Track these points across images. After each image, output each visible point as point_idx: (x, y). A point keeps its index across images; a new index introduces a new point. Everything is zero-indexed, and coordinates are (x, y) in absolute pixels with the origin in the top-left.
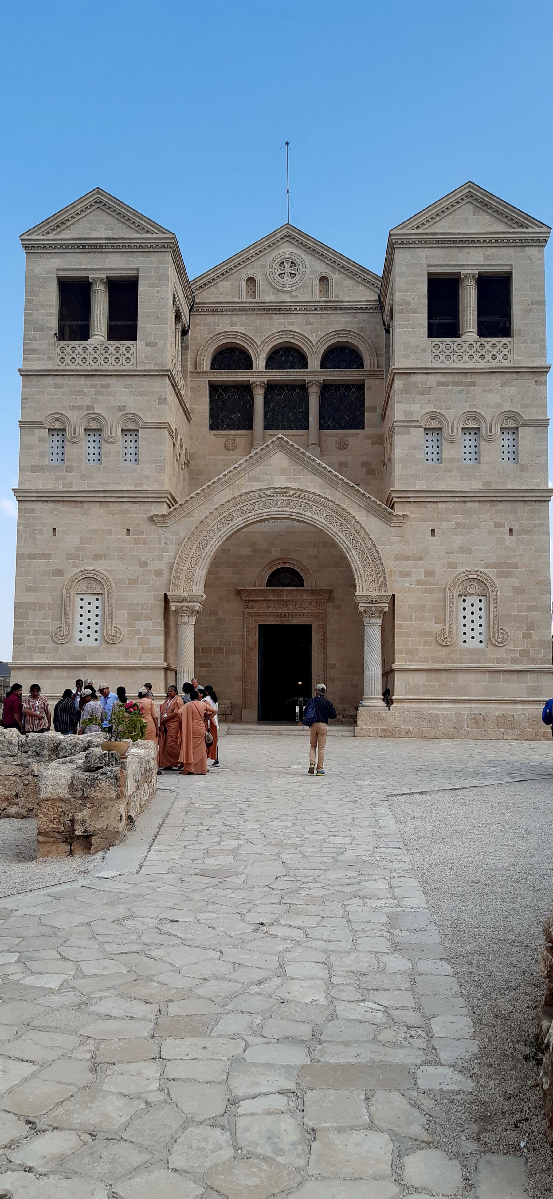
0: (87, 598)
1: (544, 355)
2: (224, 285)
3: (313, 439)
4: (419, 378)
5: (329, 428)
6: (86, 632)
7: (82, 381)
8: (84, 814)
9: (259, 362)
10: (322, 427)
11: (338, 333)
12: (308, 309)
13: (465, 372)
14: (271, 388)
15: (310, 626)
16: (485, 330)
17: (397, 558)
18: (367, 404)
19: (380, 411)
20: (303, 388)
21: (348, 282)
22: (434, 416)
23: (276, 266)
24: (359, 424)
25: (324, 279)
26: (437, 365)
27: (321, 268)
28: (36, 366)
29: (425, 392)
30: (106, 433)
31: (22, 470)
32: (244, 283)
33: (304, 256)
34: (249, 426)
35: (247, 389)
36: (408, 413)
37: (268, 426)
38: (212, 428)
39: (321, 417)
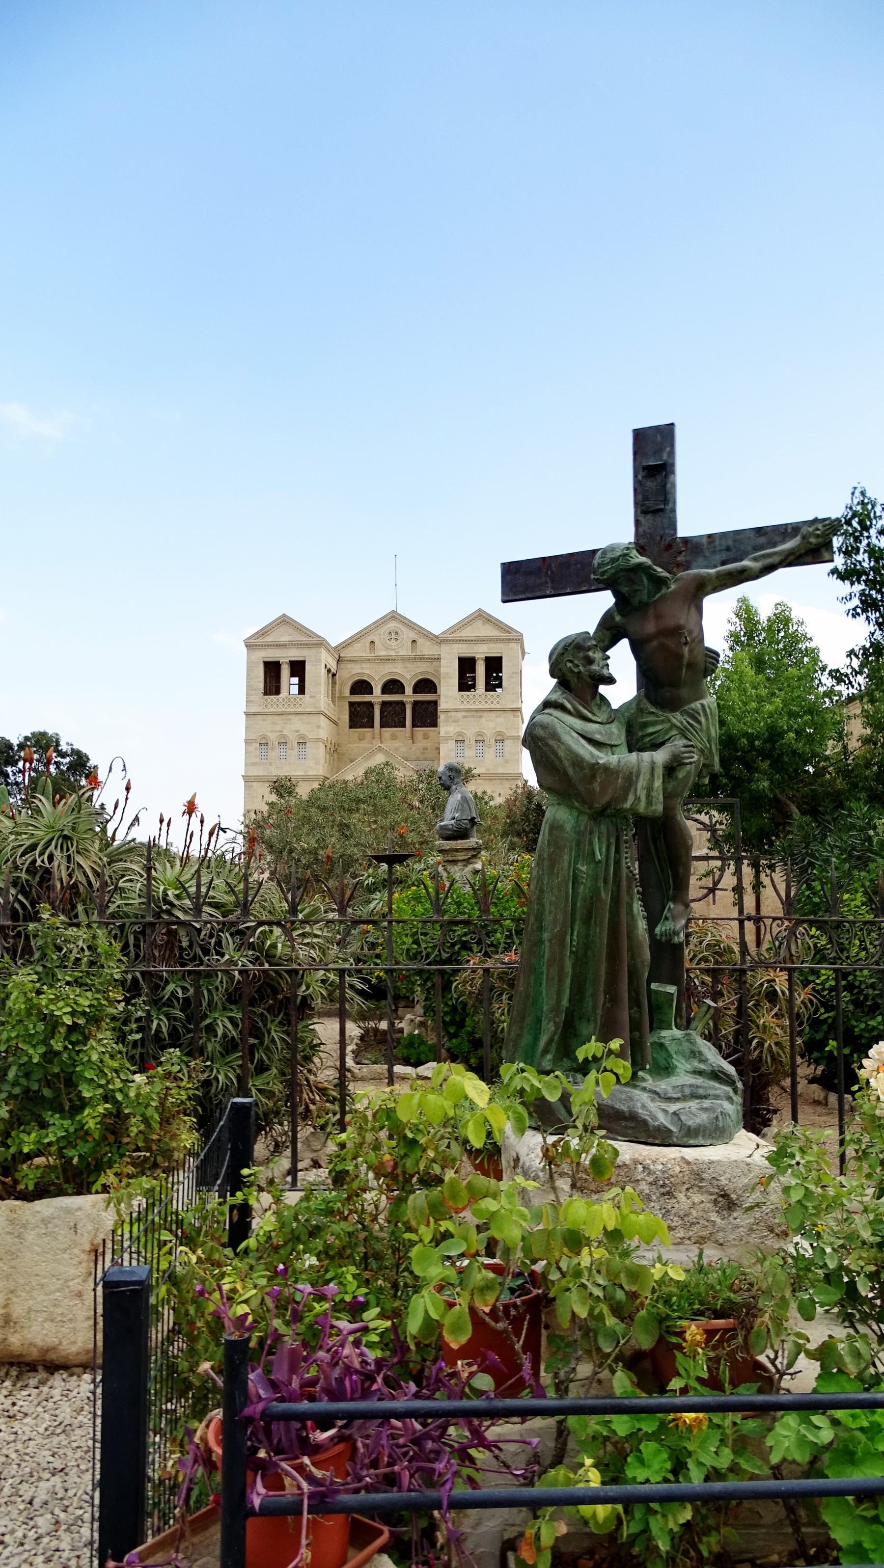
2: (357, 646)
4: (453, 714)
7: (277, 717)
10: (414, 726)
11: (422, 673)
12: (404, 659)
13: (477, 711)
14: (384, 704)
16: (490, 687)
21: (428, 643)
22: (460, 734)
25: (414, 641)
26: (462, 707)
27: (413, 635)
28: (253, 710)
29: (456, 721)
30: (289, 744)
31: (247, 765)
32: (368, 645)
33: (403, 628)
36: (447, 733)
37: (382, 726)
39: (413, 720)
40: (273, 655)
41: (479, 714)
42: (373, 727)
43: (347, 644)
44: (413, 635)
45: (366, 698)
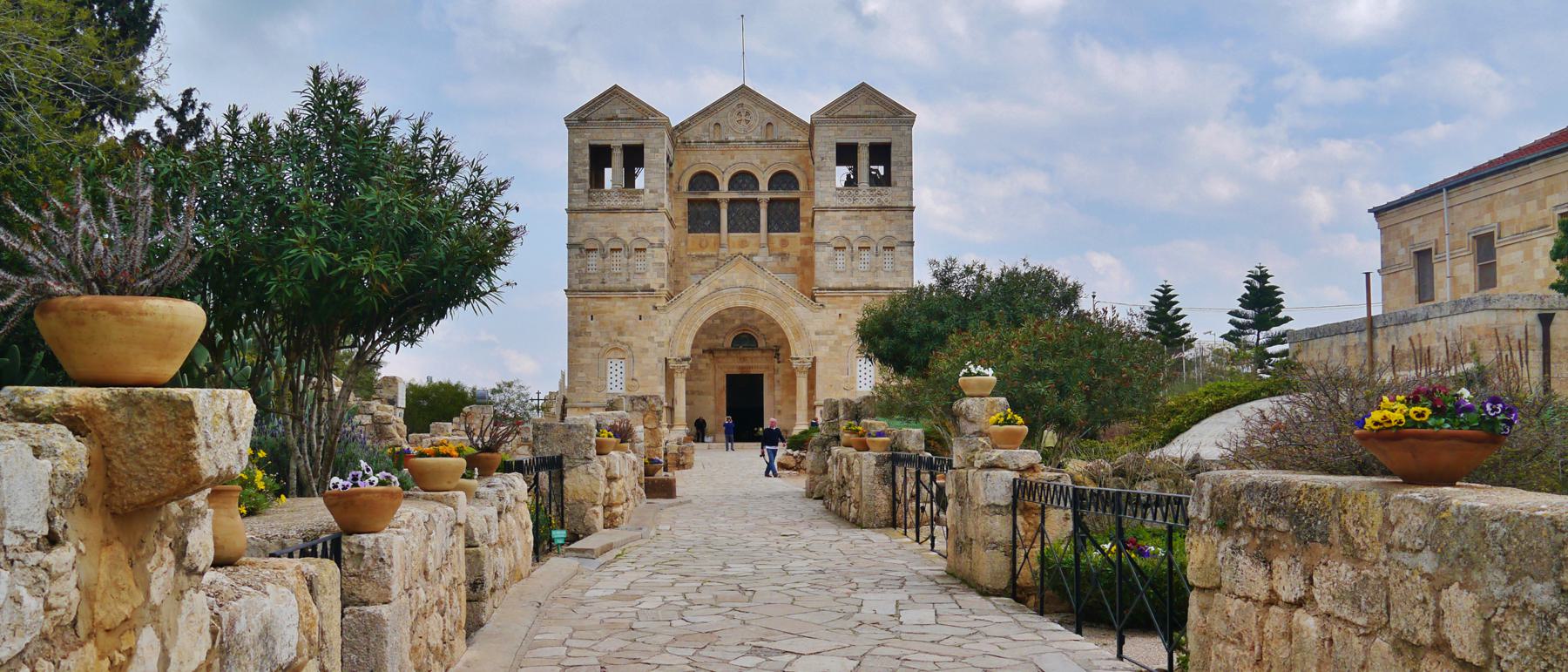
0: (614, 362)
1: (911, 199)
3: (764, 241)
5: (775, 231)
6: (614, 384)
8: (683, 458)
9: (724, 186)
10: (769, 231)
14: (732, 202)
15: (762, 375)
17: (817, 333)
18: (801, 215)
19: (810, 221)
20: (756, 202)
23: (735, 114)
24: (796, 229)
27: (768, 117)
34: (716, 228)
35: (716, 203)
38: (690, 232)
40: (602, 136)
41: (866, 214)
42: (718, 231)
43: (684, 126)
44: (768, 117)
45: (713, 195)
